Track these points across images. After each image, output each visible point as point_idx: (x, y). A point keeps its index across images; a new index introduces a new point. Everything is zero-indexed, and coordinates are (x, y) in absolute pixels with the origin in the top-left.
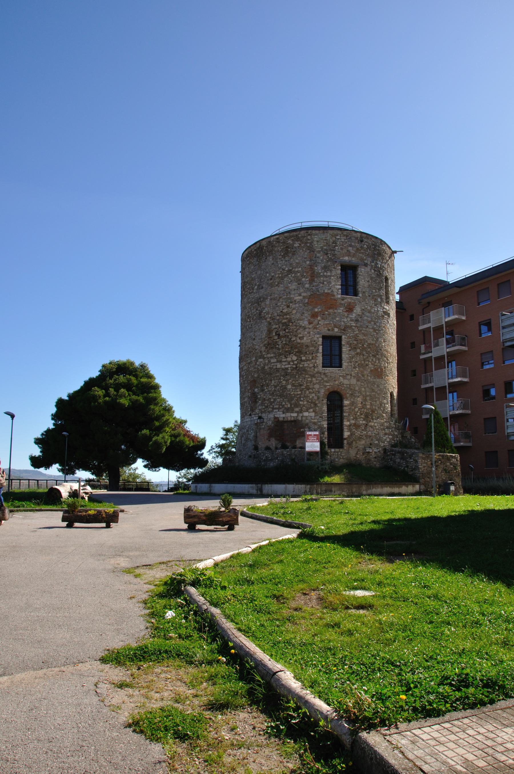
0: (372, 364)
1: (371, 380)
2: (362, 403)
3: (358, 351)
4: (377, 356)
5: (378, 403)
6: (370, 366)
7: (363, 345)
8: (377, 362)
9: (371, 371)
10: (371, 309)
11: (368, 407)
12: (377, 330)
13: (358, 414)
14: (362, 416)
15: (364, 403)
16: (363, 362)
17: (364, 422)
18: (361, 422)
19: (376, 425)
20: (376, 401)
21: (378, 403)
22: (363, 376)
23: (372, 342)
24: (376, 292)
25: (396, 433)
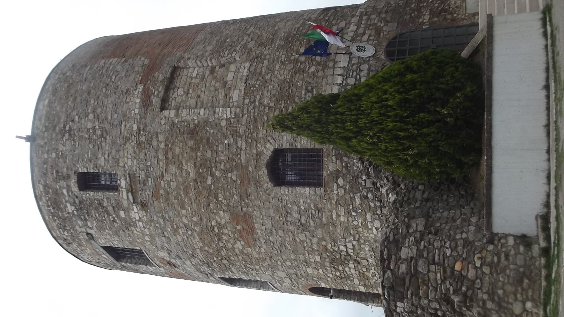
0: (235, 243)
1: (264, 246)
2: (315, 268)
3: (225, 262)
4: (216, 230)
5: (302, 237)
6: (241, 248)
7: (212, 254)
8: (226, 231)
9: (248, 244)
10: (147, 235)
11: (318, 259)
12: (172, 227)
13: (338, 274)
14: (341, 268)
15: (314, 265)
16: (240, 257)
17: (351, 266)
18: (353, 271)
19: (350, 246)
20: (302, 242)
21: (302, 237)
22: (264, 260)
23: (198, 239)
24: (114, 221)
25: (358, 201)
